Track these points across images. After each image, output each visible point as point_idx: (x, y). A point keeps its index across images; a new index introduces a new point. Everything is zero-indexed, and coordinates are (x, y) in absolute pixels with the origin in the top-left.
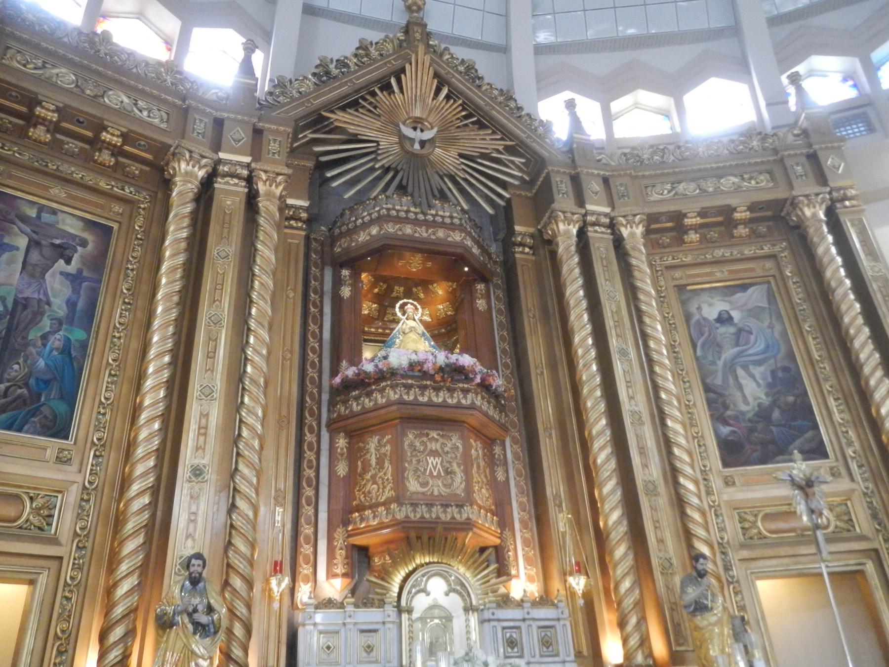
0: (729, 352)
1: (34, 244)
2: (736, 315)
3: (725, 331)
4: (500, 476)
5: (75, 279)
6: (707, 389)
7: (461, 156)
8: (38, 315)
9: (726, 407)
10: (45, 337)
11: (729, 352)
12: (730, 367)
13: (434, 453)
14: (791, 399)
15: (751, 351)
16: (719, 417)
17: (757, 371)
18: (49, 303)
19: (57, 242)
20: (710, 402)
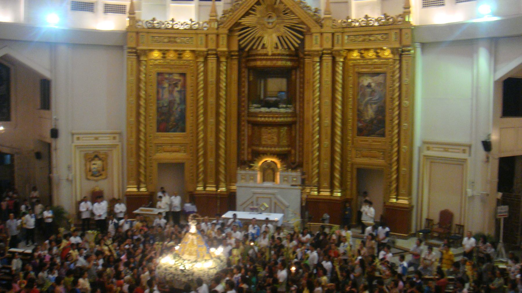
0: (368, 98)
1: (170, 85)
2: (373, 85)
3: (369, 90)
4: (294, 135)
5: (179, 92)
6: (359, 110)
7: (285, 26)
8: (174, 104)
9: (362, 117)
10: (176, 109)
11: (368, 98)
12: (366, 105)
13: (270, 133)
14: (380, 117)
15: (374, 99)
16: (359, 121)
17: (374, 106)
18: (175, 100)
19: (174, 82)
20: (358, 115)
